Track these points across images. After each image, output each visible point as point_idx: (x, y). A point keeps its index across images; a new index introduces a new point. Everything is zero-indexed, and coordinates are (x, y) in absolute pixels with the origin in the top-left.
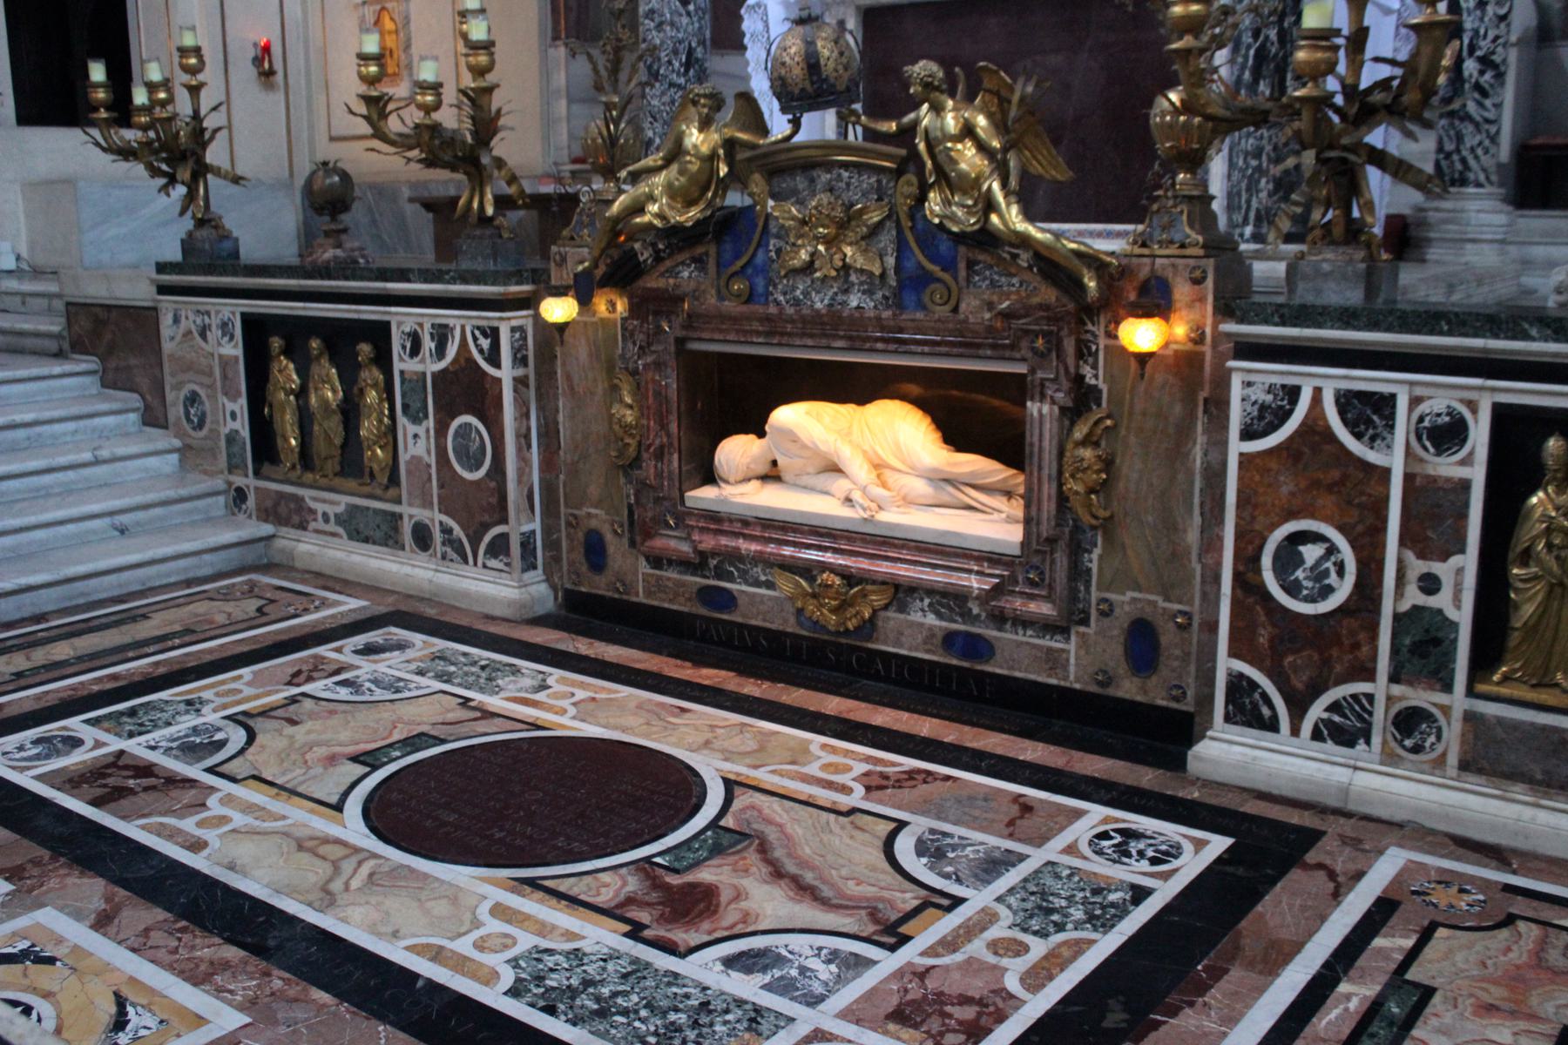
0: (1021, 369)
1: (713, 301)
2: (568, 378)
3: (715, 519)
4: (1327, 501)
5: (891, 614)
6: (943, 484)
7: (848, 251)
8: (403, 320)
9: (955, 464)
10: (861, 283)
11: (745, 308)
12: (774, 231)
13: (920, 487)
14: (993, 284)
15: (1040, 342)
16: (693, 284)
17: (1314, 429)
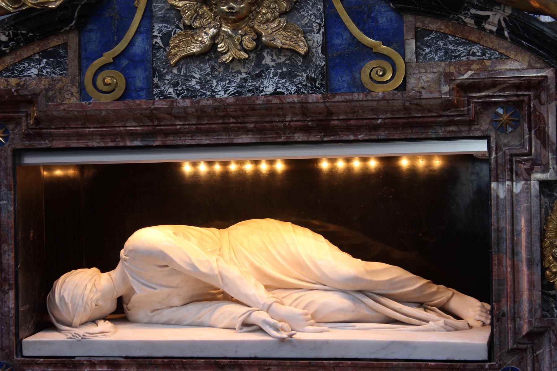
1: (74, 100)
6: (359, 296)
7: (262, 29)
9: (373, 272)
10: (279, 66)
11: (121, 105)
12: (160, 14)
13: (336, 301)
14: (448, 55)
16: (44, 83)
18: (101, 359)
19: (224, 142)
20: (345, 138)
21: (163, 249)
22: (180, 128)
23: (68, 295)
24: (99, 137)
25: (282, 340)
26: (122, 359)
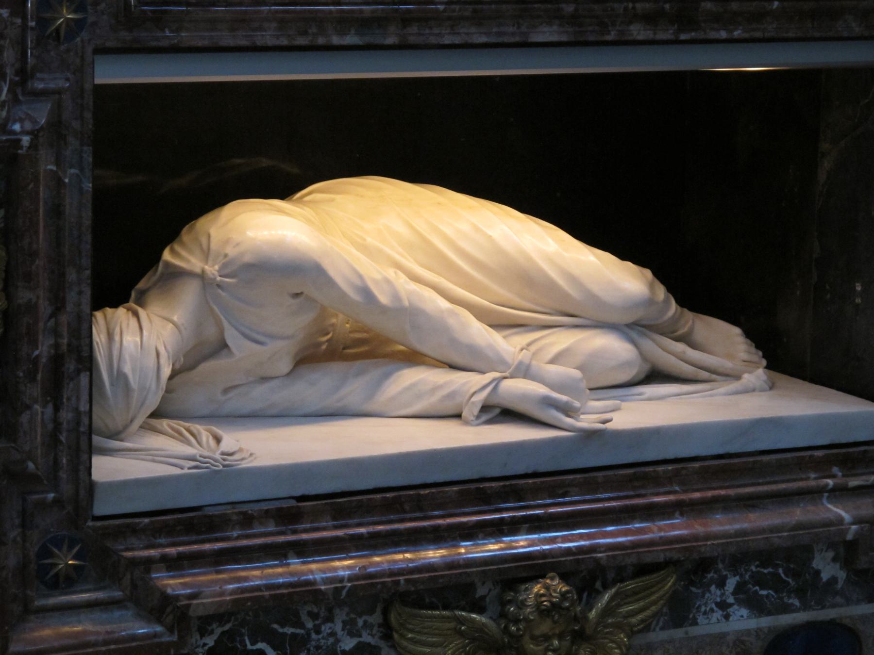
5: (658, 636)
18: (265, 506)
19: (512, 40)
20: (713, 35)
21: (318, 260)
22: (445, 11)
23: (134, 370)
24: (274, 25)
25: (590, 435)
26: (293, 503)
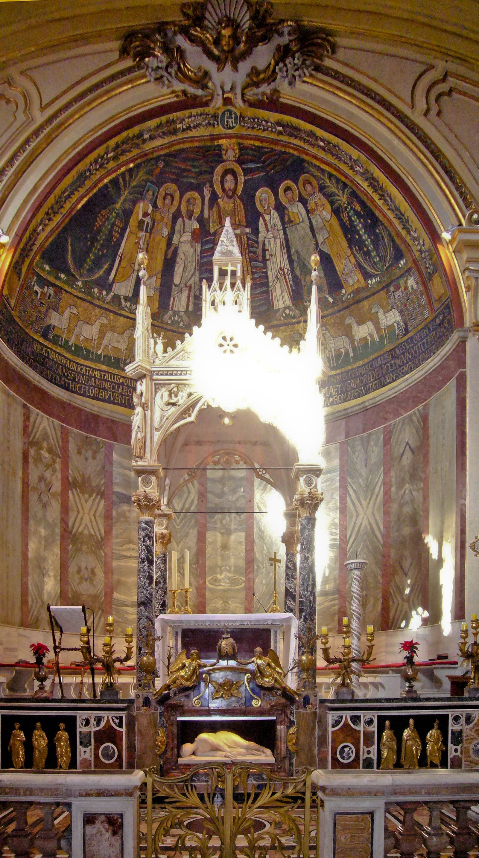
0: (274, 718)
2: (140, 731)
3: (188, 766)
4: (349, 739)
8: (81, 716)
15: (280, 712)
17: (346, 725)
